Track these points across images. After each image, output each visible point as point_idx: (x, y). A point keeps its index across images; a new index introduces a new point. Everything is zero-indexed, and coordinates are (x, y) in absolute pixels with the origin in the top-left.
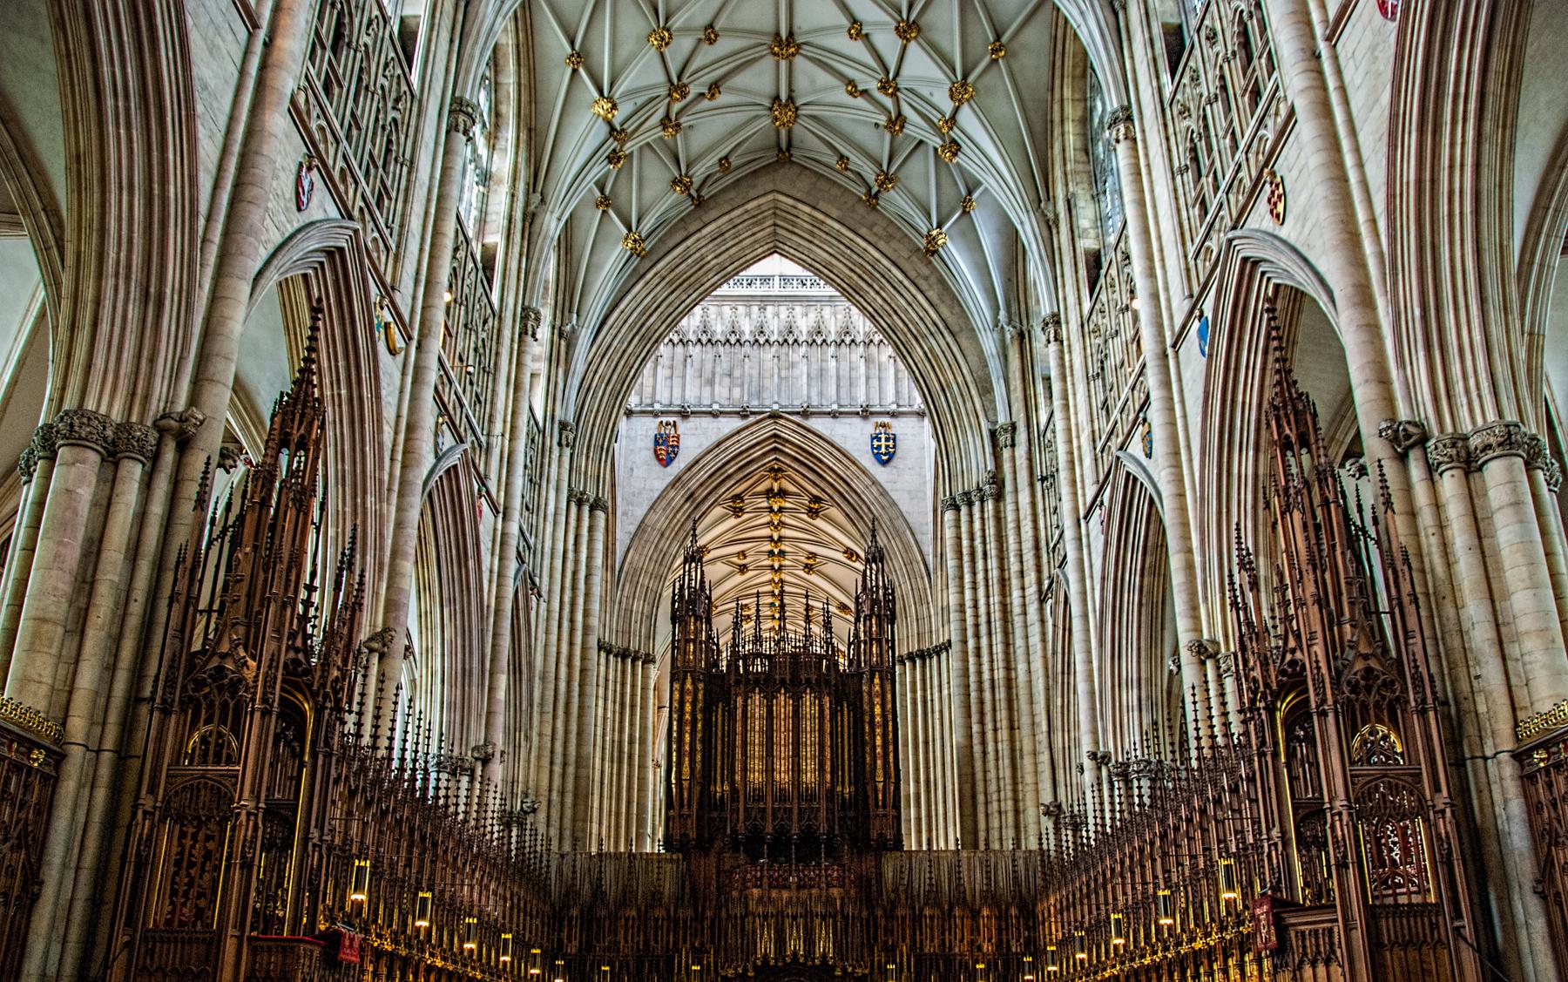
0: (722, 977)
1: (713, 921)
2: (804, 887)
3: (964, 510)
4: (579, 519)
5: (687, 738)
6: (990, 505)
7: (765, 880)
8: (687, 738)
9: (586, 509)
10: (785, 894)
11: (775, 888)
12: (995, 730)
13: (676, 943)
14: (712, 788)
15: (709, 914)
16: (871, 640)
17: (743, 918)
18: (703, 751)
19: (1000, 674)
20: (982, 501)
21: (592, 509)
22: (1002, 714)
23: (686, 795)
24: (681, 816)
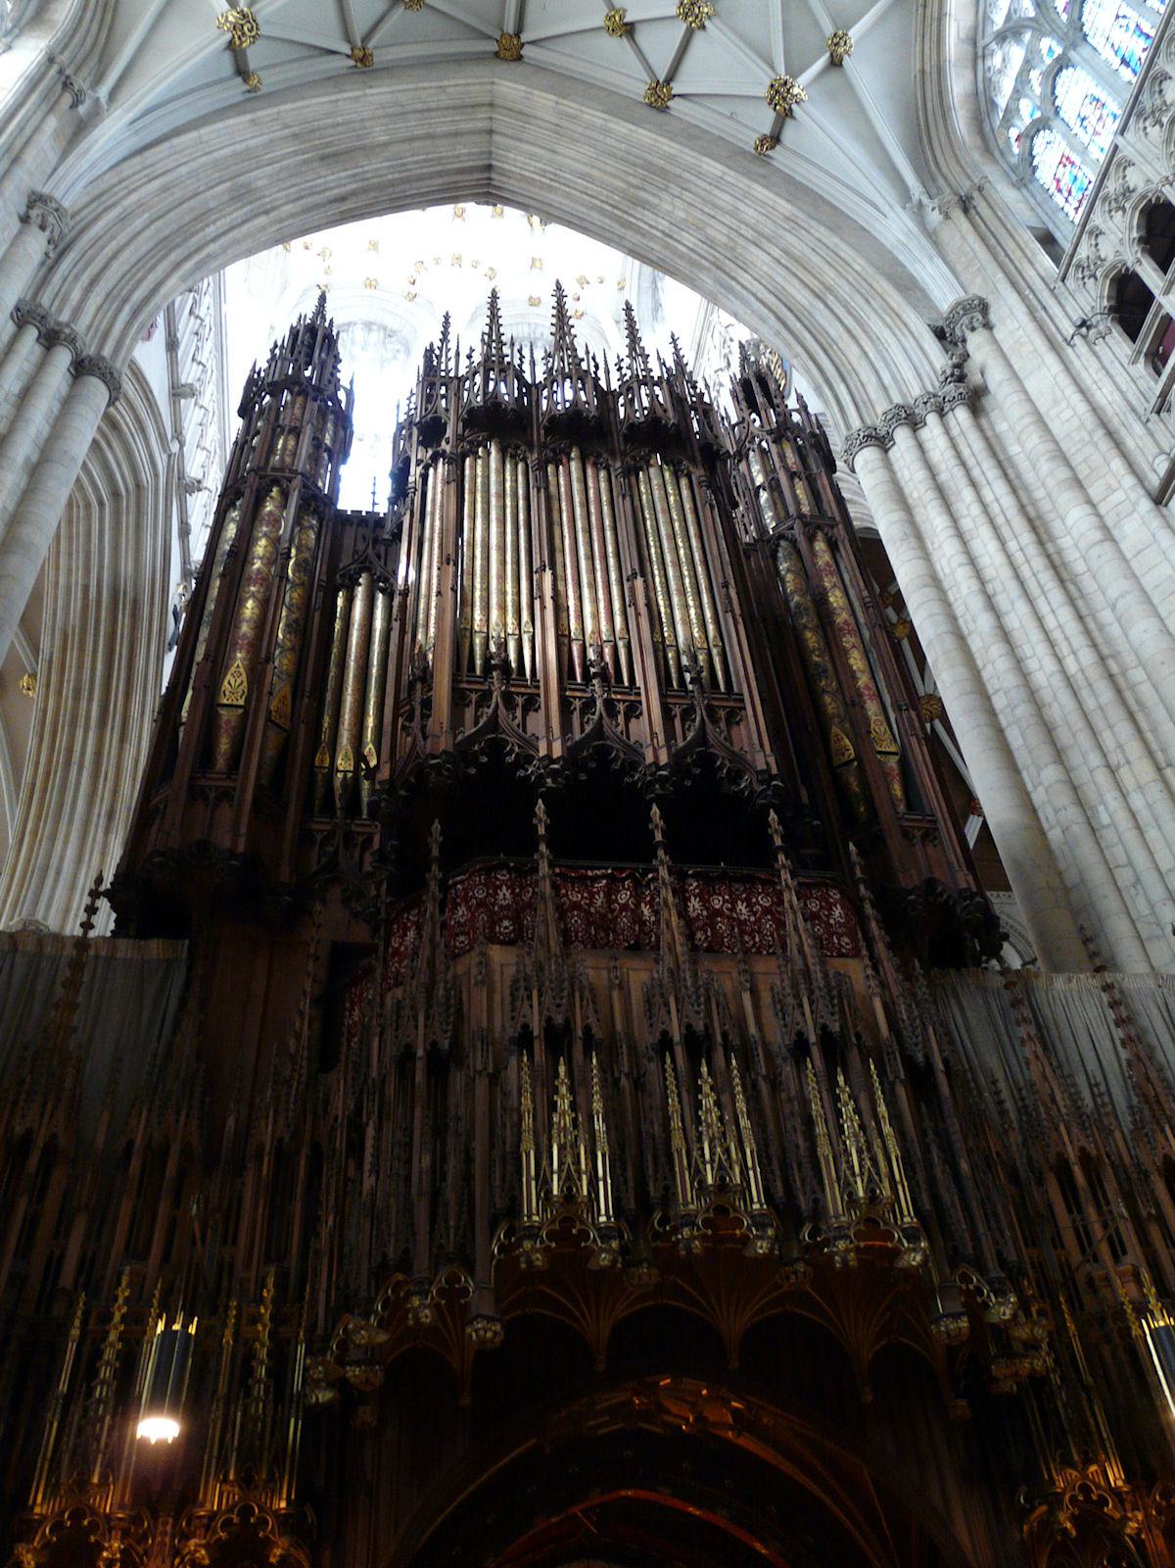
0: (314, 1416)
1: (283, 1158)
2: (714, 948)
3: (902, 435)
4: (42, 366)
5: (250, 607)
6: (961, 416)
7: (545, 924)
8: (250, 607)
9: (63, 358)
10: (639, 975)
11: (594, 944)
12: (1112, 771)
13: (86, 1265)
14: (322, 759)
15: (267, 1133)
16: (792, 476)
17: (441, 1064)
18: (301, 651)
19: (1081, 660)
20: (941, 413)
21: (81, 368)
22: (1118, 734)
23: (224, 744)
24: (195, 793)
